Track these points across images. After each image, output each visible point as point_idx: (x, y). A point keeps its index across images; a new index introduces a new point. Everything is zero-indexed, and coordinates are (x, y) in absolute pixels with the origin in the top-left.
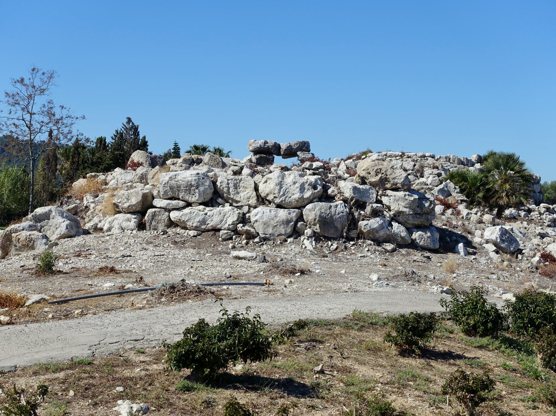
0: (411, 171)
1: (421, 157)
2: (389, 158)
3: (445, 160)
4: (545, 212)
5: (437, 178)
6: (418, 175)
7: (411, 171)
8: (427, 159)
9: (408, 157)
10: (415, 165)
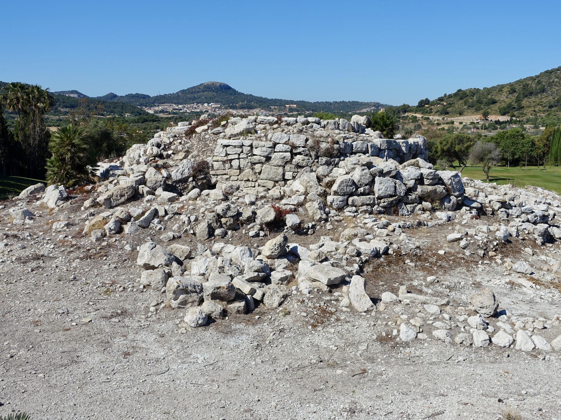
1: (303, 124)
3: (333, 127)
4: (500, 208)
5: (367, 171)
6: (313, 154)
7: (302, 149)
8: (312, 127)
9: (288, 124)
10: (307, 140)
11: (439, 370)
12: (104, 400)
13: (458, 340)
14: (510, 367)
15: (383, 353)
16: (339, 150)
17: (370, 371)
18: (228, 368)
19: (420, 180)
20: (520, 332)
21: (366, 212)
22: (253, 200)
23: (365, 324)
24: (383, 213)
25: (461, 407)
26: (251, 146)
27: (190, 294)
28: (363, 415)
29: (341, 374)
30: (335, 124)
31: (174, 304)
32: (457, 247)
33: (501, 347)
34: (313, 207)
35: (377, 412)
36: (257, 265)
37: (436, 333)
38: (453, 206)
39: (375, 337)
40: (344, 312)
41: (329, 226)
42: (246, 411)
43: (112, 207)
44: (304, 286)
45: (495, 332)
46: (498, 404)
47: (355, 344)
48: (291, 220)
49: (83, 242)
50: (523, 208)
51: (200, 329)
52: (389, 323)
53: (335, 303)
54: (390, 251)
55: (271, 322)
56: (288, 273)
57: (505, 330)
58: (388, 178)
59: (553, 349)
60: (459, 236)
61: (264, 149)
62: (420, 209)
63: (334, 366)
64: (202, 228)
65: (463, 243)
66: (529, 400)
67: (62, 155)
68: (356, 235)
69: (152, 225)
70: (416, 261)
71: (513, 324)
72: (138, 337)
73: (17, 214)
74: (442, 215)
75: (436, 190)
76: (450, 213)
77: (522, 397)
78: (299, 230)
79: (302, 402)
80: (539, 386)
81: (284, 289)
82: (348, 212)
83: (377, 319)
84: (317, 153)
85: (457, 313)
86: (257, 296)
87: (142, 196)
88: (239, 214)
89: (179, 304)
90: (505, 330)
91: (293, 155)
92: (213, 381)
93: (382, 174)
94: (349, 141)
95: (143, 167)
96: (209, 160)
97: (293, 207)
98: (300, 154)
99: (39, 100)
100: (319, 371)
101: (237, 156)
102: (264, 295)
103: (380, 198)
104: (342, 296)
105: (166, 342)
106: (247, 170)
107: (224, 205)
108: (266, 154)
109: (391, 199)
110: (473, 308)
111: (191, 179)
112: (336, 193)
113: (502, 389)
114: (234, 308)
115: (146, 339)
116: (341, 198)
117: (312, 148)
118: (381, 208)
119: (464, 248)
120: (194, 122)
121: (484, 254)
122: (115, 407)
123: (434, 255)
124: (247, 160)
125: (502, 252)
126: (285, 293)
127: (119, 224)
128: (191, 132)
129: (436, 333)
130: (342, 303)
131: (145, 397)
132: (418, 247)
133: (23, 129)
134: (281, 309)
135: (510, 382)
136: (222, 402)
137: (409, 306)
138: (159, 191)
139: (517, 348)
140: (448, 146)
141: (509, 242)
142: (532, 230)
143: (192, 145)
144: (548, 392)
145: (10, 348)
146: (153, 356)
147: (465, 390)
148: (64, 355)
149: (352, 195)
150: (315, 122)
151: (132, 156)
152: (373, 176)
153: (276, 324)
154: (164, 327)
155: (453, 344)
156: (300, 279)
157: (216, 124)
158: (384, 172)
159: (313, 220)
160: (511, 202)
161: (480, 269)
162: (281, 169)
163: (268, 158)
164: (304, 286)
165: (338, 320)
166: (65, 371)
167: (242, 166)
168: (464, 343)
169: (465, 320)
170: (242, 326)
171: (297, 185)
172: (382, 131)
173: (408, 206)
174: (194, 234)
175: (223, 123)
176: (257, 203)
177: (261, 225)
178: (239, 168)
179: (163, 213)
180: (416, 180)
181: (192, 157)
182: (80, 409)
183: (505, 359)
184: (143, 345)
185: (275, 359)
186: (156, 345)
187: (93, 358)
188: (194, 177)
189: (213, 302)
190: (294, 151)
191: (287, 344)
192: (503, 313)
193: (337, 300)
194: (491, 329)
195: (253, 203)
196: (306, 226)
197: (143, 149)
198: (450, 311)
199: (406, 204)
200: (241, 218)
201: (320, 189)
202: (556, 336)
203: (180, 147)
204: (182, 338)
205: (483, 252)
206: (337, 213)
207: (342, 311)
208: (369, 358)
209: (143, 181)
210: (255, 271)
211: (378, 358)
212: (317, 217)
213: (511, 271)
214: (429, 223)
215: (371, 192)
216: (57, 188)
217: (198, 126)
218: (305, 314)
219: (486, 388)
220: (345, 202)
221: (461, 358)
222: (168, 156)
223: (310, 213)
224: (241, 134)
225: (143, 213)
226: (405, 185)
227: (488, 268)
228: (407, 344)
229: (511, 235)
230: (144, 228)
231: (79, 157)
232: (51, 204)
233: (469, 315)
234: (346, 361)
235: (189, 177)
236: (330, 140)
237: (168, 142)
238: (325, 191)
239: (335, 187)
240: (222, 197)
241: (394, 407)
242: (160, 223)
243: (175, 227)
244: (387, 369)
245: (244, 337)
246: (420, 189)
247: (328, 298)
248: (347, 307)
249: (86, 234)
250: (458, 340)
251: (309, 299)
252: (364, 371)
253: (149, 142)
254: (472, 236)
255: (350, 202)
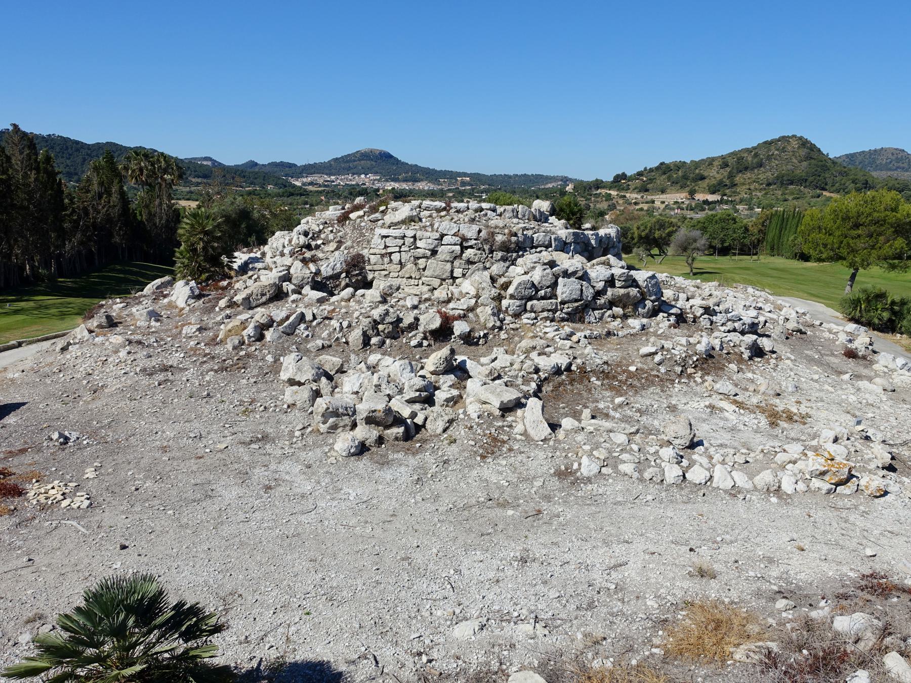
0: (474, 242)
1: (476, 211)
2: (427, 213)
3: (511, 214)
4: (702, 314)
5: (549, 271)
6: (486, 247)
7: (474, 242)
8: (486, 214)
9: (458, 211)
10: (480, 231)
11: (624, 512)
12: (242, 544)
13: (647, 475)
14: (705, 508)
15: (561, 490)
16: (517, 243)
17: (545, 512)
18: (384, 507)
19: (611, 282)
20: (718, 466)
21: (546, 319)
22: (416, 303)
23: (541, 455)
24: (567, 320)
25: (647, 557)
26: (414, 237)
27: (342, 417)
28: (536, 565)
29: (513, 516)
30: (513, 211)
31: (323, 428)
32: (651, 363)
33: (695, 484)
34: (485, 313)
35: (552, 561)
36: (419, 383)
37: (623, 468)
38: (648, 312)
39: (552, 471)
40: (518, 441)
41: (503, 335)
42: (403, 559)
43: (251, 308)
44: (473, 409)
45: (689, 467)
46: (689, 555)
47: (529, 480)
48: (460, 327)
49: (218, 350)
50: (729, 315)
51: (352, 458)
52: (570, 455)
53: (508, 429)
54: (574, 368)
55: (434, 451)
56: (455, 392)
57: (701, 465)
58: (573, 279)
59: (755, 486)
60: (653, 350)
61: (430, 241)
62: (609, 316)
63: (504, 505)
64: (355, 336)
65: (658, 358)
66: (725, 549)
67: (193, 245)
68: (534, 348)
69: (297, 331)
70: (604, 379)
71: (711, 458)
72: (281, 468)
73: (141, 315)
74: (635, 323)
75: (628, 293)
76: (645, 321)
77: (717, 545)
78: (468, 339)
79: (467, 548)
80: (737, 531)
81: (449, 413)
82: (526, 319)
83: (555, 449)
84: (491, 246)
85: (647, 443)
86: (419, 420)
87: (287, 295)
88: (399, 320)
89: (329, 428)
90: (701, 465)
91: (463, 248)
92: (366, 522)
93: (566, 274)
94: (529, 233)
95: (288, 261)
96: (365, 252)
97: (462, 312)
98: (471, 247)
99: (165, 171)
100: (488, 511)
101: (397, 249)
102: (426, 419)
103: (563, 303)
104: (516, 422)
105: (313, 474)
106: (410, 266)
107: (381, 309)
108: (431, 247)
109: (576, 304)
110: (666, 438)
111: (344, 275)
112: (512, 297)
113: (694, 535)
114: (392, 434)
115: (291, 470)
116: (518, 303)
117: (486, 241)
118: (564, 315)
119: (659, 365)
120: (348, 206)
121: (682, 371)
122: (255, 552)
123: (624, 371)
124: (410, 254)
125: (702, 369)
126: (451, 417)
127: (259, 331)
128: (344, 218)
129: (623, 468)
130: (516, 430)
131: (288, 541)
132: (606, 363)
133: (147, 206)
134: (445, 436)
135: (704, 527)
136: (377, 548)
137: (594, 435)
138: (307, 290)
139: (714, 485)
140: (647, 231)
141: (711, 356)
142: (738, 343)
143: (346, 234)
144: (747, 540)
145: (134, 479)
146: (298, 490)
147: (652, 536)
148: (196, 488)
149: (530, 298)
150: (490, 209)
151: (274, 246)
152: (556, 277)
153: (440, 454)
154: (311, 456)
155: (641, 480)
156: (468, 401)
157: (374, 210)
158: (569, 272)
159: (486, 328)
160: (716, 308)
161: (676, 390)
162: (449, 265)
163: (434, 252)
164: (473, 409)
165: (510, 450)
166: (198, 507)
167: (403, 261)
168: (654, 479)
169: (657, 452)
170: (400, 456)
171: (467, 286)
172: (568, 220)
173: (596, 312)
174: (347, 343)
175: (382, 208)
176: (421, 306)
177: (425, 333)
178: (400, 263)
179: (311, 318)
180: (606, 282)
181: (346, 248)
182: (215, 555)
183: (700, 499)
184: (287, 477)
185: (438, 496)
186: (302, 477)
187: (229, 492)
188: (348, 272)
189: (367, 427)
190: (465, 244)
191: (452, 478)
192: (700, 443)
193: (510, 426)
194: (685, 463)
195: (415, 307)
196: (477, 335)
197: (287, 238)
198: (640, 441)
199: (594, 310)
200: (401, 325)
201: (494, 292)
202: (759, 472)
203: (331, 237)
204: (332, 469)
205: (680, 369)
206: (513, 320)
207: (515, 439)
208: (545, 496)
209: (287, 278)
210: (417, 391)
211: (555, 496)
212: (490, 325)
213: (712, 392)
214: (620, 333)
215: (556, 296)
216: (187, 284)
217: (352, 212)
218: (473, 443)
219: (676, 533)
220: (523, 307)
221: (649, 498)
222: (318, 247)
223: (482, 320)
224: (403, 222)
225: (288, 318)
226: (593, 287)
227: (685, 389)
228: (589, 480)
229: (713, 349)
230: (288, 335)
231: (213, 247)
232: (181, 303)
233: (661, 446)
234: (519, 499)
235: (341, 273)
236: (506, 231)
237: (317, 229)
238: (500, 294)
239: (511, 290)
240: (380, 299)
241: (571, 556)
242: (306, 329)
243: (325, 334)
244: (564, 510)
245: (403, 469)
246: (610, 292)
247: (500, 424)
248: (521, 435)
249: (221, 341)
250: (647, 475)
251: (478, 425)
252: (539, 512)
253: (295, 230)
254: (668, 350)
255: (528, 308)
